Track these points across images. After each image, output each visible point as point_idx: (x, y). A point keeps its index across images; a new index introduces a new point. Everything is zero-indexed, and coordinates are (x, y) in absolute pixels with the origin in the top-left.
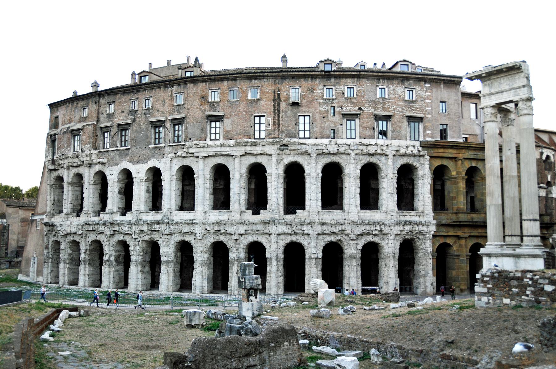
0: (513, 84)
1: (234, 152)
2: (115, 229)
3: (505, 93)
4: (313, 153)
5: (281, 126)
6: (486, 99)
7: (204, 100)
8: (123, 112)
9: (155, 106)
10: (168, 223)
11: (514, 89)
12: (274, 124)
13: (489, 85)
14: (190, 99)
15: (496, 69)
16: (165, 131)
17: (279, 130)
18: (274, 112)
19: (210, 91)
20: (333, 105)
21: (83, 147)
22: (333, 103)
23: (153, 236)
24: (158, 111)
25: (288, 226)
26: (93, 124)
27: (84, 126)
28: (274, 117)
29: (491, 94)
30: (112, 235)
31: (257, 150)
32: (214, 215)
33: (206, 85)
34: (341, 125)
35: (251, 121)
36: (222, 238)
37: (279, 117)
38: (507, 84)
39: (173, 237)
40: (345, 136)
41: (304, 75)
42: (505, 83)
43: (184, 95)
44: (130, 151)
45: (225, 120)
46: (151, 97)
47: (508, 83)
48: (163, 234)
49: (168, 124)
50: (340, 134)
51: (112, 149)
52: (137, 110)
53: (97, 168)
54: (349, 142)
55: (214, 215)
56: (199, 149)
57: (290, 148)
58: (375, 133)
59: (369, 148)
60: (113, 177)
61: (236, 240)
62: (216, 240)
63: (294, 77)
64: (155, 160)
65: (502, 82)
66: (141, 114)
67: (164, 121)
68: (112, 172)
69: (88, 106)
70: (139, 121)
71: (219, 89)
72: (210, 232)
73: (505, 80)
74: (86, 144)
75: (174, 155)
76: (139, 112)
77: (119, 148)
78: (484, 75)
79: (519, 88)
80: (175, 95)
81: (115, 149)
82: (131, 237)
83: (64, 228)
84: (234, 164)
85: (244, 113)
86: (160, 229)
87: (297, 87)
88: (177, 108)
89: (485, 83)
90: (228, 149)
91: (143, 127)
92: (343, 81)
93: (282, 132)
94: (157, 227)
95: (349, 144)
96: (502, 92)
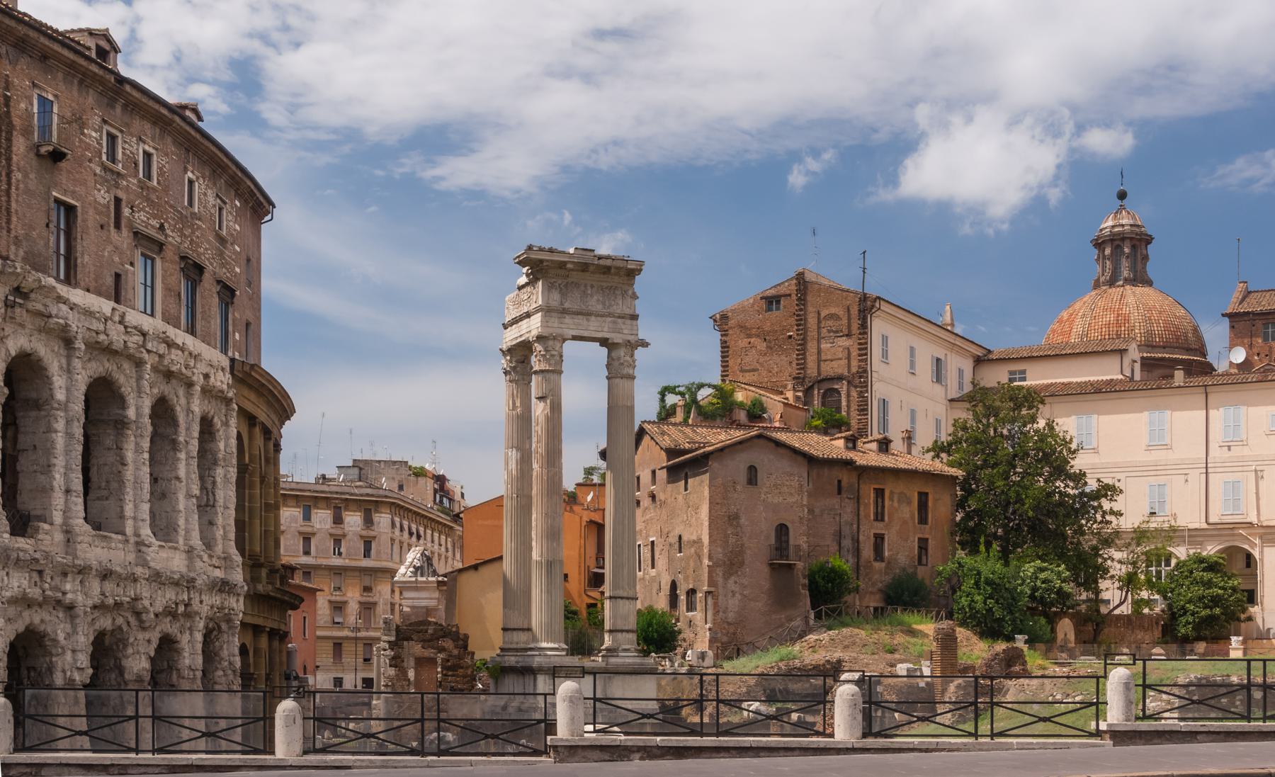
0: (611, 305)
3: (593, 318)
4: (80, 336)
6: (553, 319)
11: (614, 316)
13: (561, 290)
15: (601, 262)
25: (35, 576)
29: (564, 312)
34: (132, 264)
38: (598, 300)
42: (595, 297)
47: (601, 299)
50: (130, 296)
54: (147, 323)
57: (30, 305)
58: (182, 311)
59: (175, 355)
65: (589, 292)
73: (595, 289)
78: (569, 266)
79: (623, 318)
89: (553, 280)
93: (17, 241)
95: (145, 328)
96: (588, 314)
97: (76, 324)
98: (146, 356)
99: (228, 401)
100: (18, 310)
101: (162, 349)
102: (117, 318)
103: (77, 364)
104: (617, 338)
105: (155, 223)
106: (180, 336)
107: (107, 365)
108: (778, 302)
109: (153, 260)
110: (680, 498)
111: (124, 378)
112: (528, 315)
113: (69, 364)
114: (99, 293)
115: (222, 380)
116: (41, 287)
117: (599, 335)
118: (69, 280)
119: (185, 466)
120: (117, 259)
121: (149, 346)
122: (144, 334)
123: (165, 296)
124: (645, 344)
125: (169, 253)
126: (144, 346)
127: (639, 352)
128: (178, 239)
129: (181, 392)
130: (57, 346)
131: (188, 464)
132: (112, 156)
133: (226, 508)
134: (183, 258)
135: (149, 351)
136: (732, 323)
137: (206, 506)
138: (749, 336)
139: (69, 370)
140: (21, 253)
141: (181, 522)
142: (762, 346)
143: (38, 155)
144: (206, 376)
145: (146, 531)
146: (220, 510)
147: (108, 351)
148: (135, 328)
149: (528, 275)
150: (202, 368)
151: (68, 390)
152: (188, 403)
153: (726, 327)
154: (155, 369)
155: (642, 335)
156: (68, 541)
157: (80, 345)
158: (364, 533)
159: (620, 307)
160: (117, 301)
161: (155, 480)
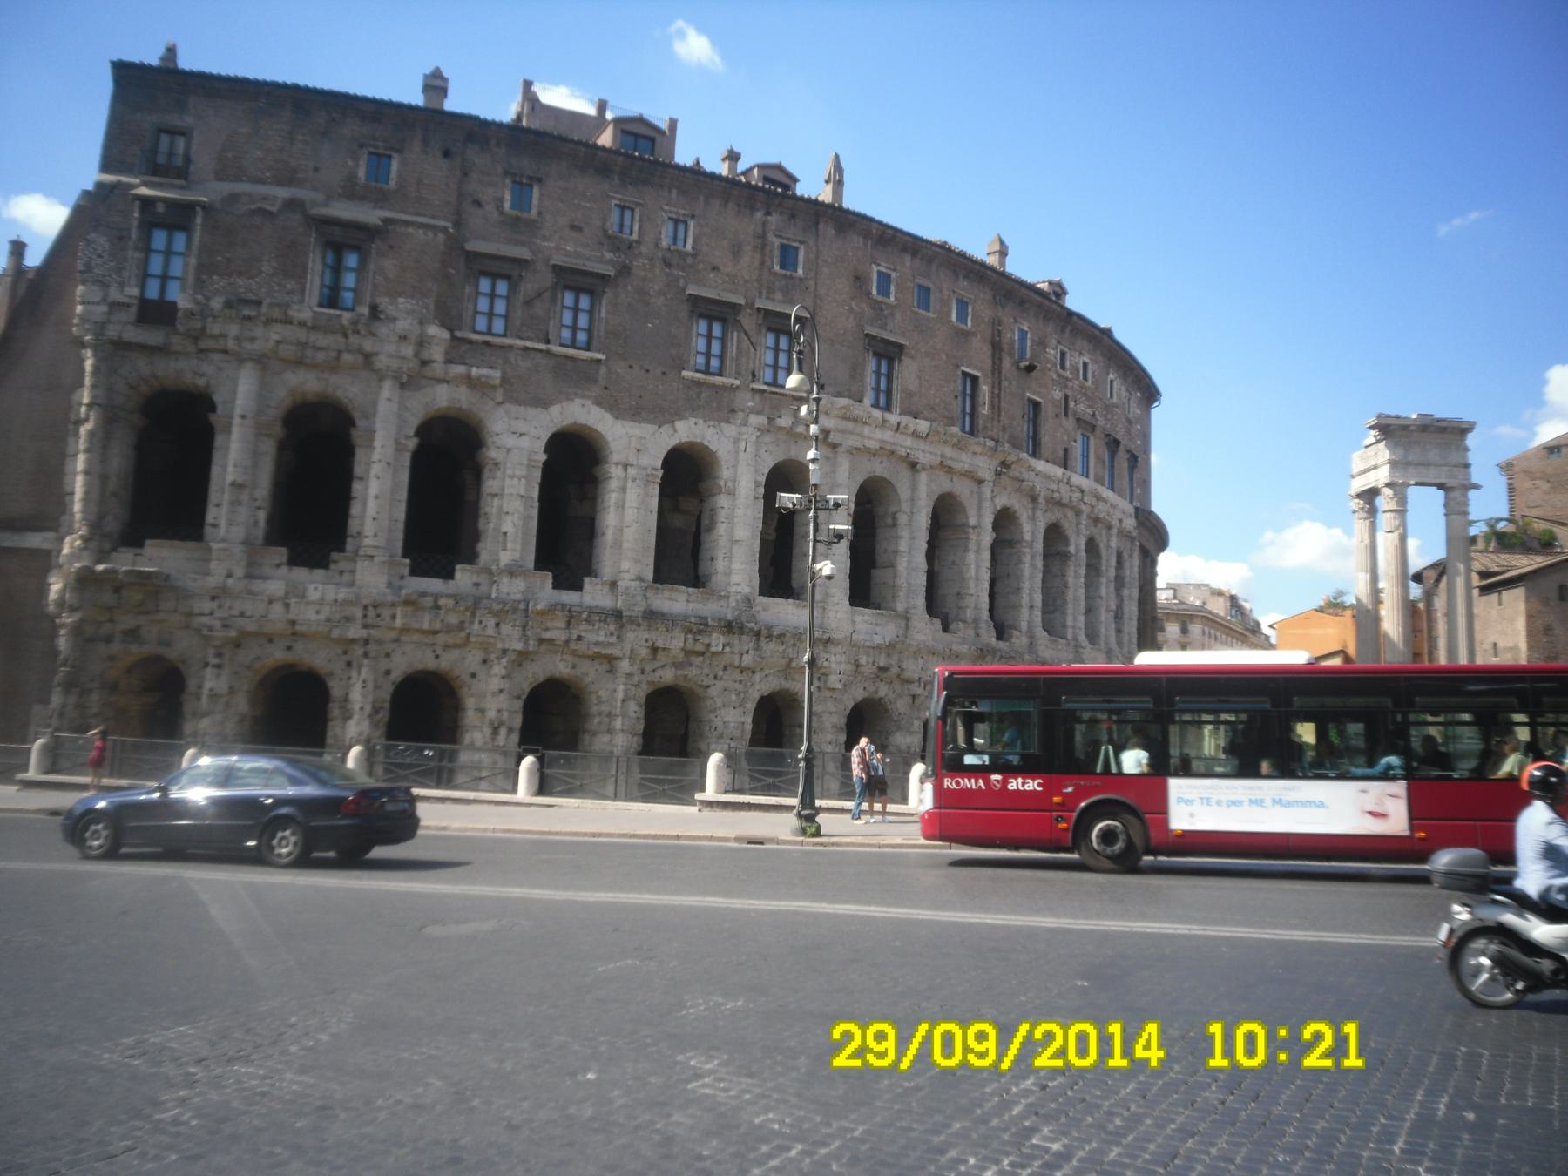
1: (921, 454)
2: (547, 635)
4: (1042, 494)
5: (1003, 413)
7: (861, 287)
8: (574, 227)
9: (705, 249)
10: (758, 634)
12: (992, 406)
14: (826, 270)
15: (1440, 424)
16: (739, 342)
17: (999, 421)
18: (993, 374)
19: (875, 268)
20: (1069, 393)
21: (383, 302)
22: (1066, 386)
23: (692, 672)
24: (715, 269)
26: (444, 230)
27: (387, 221)
28: (993, 387)
30: (523, 657)
31: (962, 461)
32: (866, 622)
33: (865, 244)
34: (1075, 441)
35: (955, 381)
36: (883, 691)
37: (1000, 389)
39: (757, 677)
40: (1079, 468)
41: (1040, 306)
43: (807, 253)
44: (603, 370)
45: (906, 360)
46: (693, 217)
48: (725, 668)
49: (748, 321)
51: (529, 344)
52: (639, 242)
53: (443, 397)
55: (866, 622)
56: (844, 422)
57: (1012, 473)
60: (524, 442)
61: (914, 697)
62: (866, 695)
63: (1022, 303)
64: (701, 421)
66: (651, 259)
67: (735, 308)
68: (521, 426)
69: (399, 151)
70: (644, 279)
71: (894, 270)
72: (862, 669)
74: (400, 294)
75: (761, 420)
76: (643, 249)
77: (556, 349)
78: (1412, 428)
80: (777, 242)
81: (542, 346)
82: (606, 667)
83: (238, 606)
84: (914, 488)
85: (943, 356)
86: (727, 649)
87: (1026, 329)
88: (783, 283)
90: (909, 442)
91: (659, 302)
92: (1082, 344)
94: (717, 641)
97: (1041, 488)
98: (1084, 507)
99: (1132, 539)
100: (1003, 477)
101: (1094, 501)
102: (1065, 481)
103: (1039, 513)
104: (1450, 482)
105: (1089, 411)
106: (1105, 492)
107: (1057, 514)
108: (1559, 451)
109: (1088, 438)
110: (1494, 612)
111: (1069, 526)
112: (1375, 467)
113: (1034, 514)
114: (1055, 463)
115: (1130, 523)
116: (1019, 460)
117: (1437, 481)
118: (1035, 454)
119: (1105, 589)
120: (1065, 438)
121: (1086, 500)
122: (1082, 492)
123: (1096, 463)
124: (1476, 487)
125: (1098, 431)
126: (1082, 500)
127: (1472, 494)
128: (1104, 422)
129: (1104, 532)
130: (1026, 501)
131: (1107, 587)
132: (1063, 367)
133: (1131, 619)
134: (1108, 435)
135: (1085, 503)
136: (1516, 469)
137: (1118, 616)
138: (1534, 479)
139: (1033, 519)
140: (1006, 437)
141: (1103, 630)
142: (1545, 486)
143: (1018, 368)
144: (1121, 521)
145: (1082, 638)
146: (1126, 621)
147: (1059, 504)
148: (1077, 487)
149: (1375, 436)
150: (1118, 515)
151: (1033, 533)
152: (1108, 541)
153: (1510, 473)
154: (1089, 517)
155: (1475, 479)
156: (1031, 644)
157: (1041, 500)
158: (1182, 640)
159: (1454, 457)
160: (1066, 468)
161: (1087, 598)
